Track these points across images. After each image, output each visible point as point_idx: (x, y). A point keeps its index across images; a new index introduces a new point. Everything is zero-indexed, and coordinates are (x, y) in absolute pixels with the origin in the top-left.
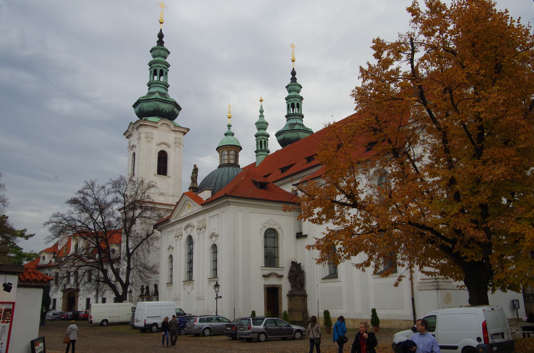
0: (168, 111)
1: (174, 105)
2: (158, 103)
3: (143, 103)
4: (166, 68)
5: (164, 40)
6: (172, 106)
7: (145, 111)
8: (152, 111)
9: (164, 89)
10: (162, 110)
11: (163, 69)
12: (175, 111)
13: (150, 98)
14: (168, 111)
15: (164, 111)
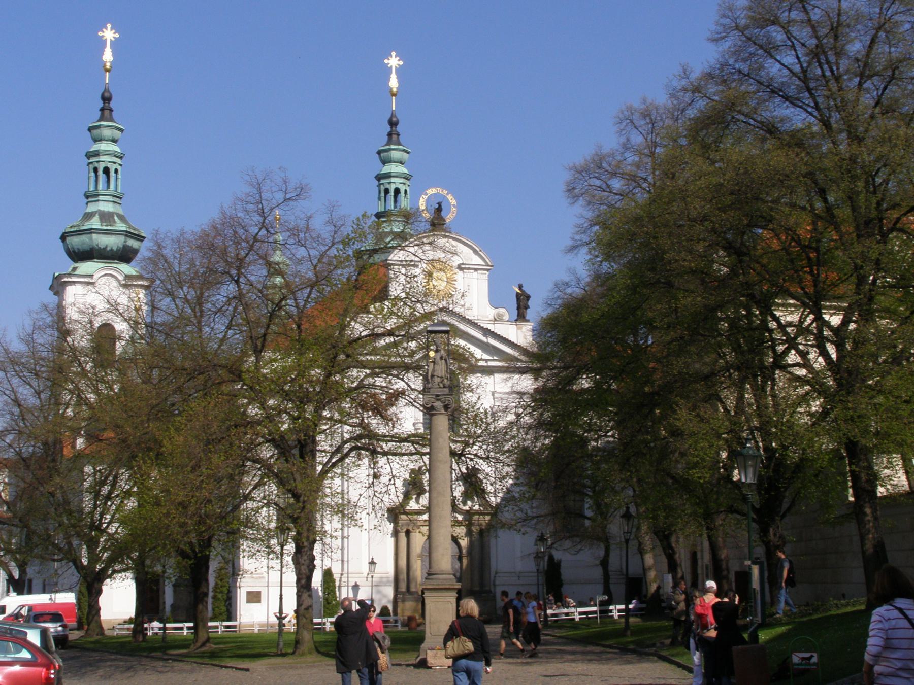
0: (115, 249)
1: (126, 236)
2: (95, 236)
3: (71, 238)
4: (115, 163)
5: (112, 104)
6: (122, 238)
7: (76, 251)
8: (87, 252)
9: (111, 204)
10: (105, 249)
11: (109, 165)
12: (130, 245)
13: (82, 228)
14: (115, 249)
15: (108, 249)
